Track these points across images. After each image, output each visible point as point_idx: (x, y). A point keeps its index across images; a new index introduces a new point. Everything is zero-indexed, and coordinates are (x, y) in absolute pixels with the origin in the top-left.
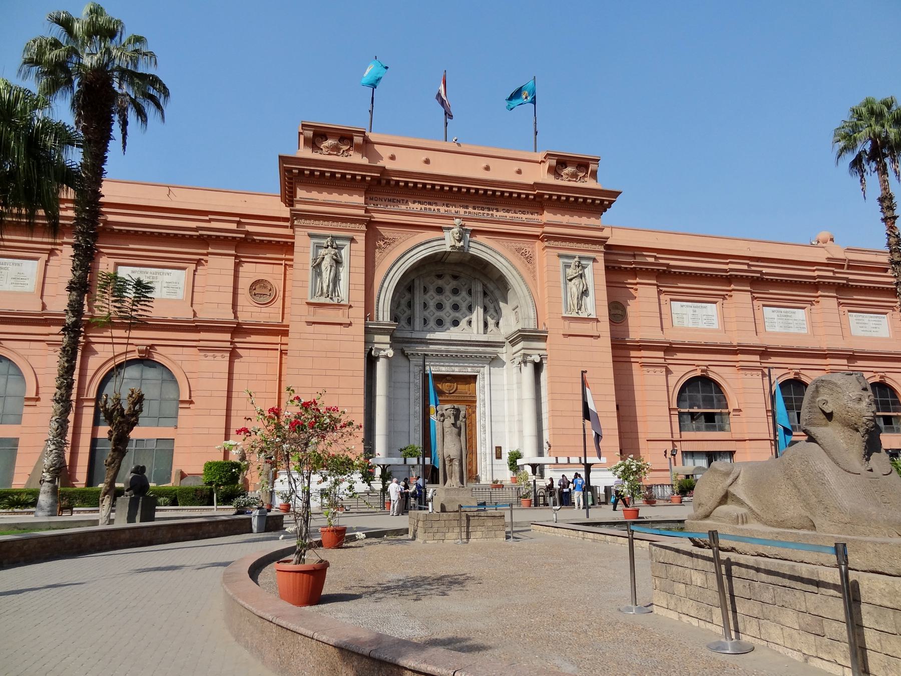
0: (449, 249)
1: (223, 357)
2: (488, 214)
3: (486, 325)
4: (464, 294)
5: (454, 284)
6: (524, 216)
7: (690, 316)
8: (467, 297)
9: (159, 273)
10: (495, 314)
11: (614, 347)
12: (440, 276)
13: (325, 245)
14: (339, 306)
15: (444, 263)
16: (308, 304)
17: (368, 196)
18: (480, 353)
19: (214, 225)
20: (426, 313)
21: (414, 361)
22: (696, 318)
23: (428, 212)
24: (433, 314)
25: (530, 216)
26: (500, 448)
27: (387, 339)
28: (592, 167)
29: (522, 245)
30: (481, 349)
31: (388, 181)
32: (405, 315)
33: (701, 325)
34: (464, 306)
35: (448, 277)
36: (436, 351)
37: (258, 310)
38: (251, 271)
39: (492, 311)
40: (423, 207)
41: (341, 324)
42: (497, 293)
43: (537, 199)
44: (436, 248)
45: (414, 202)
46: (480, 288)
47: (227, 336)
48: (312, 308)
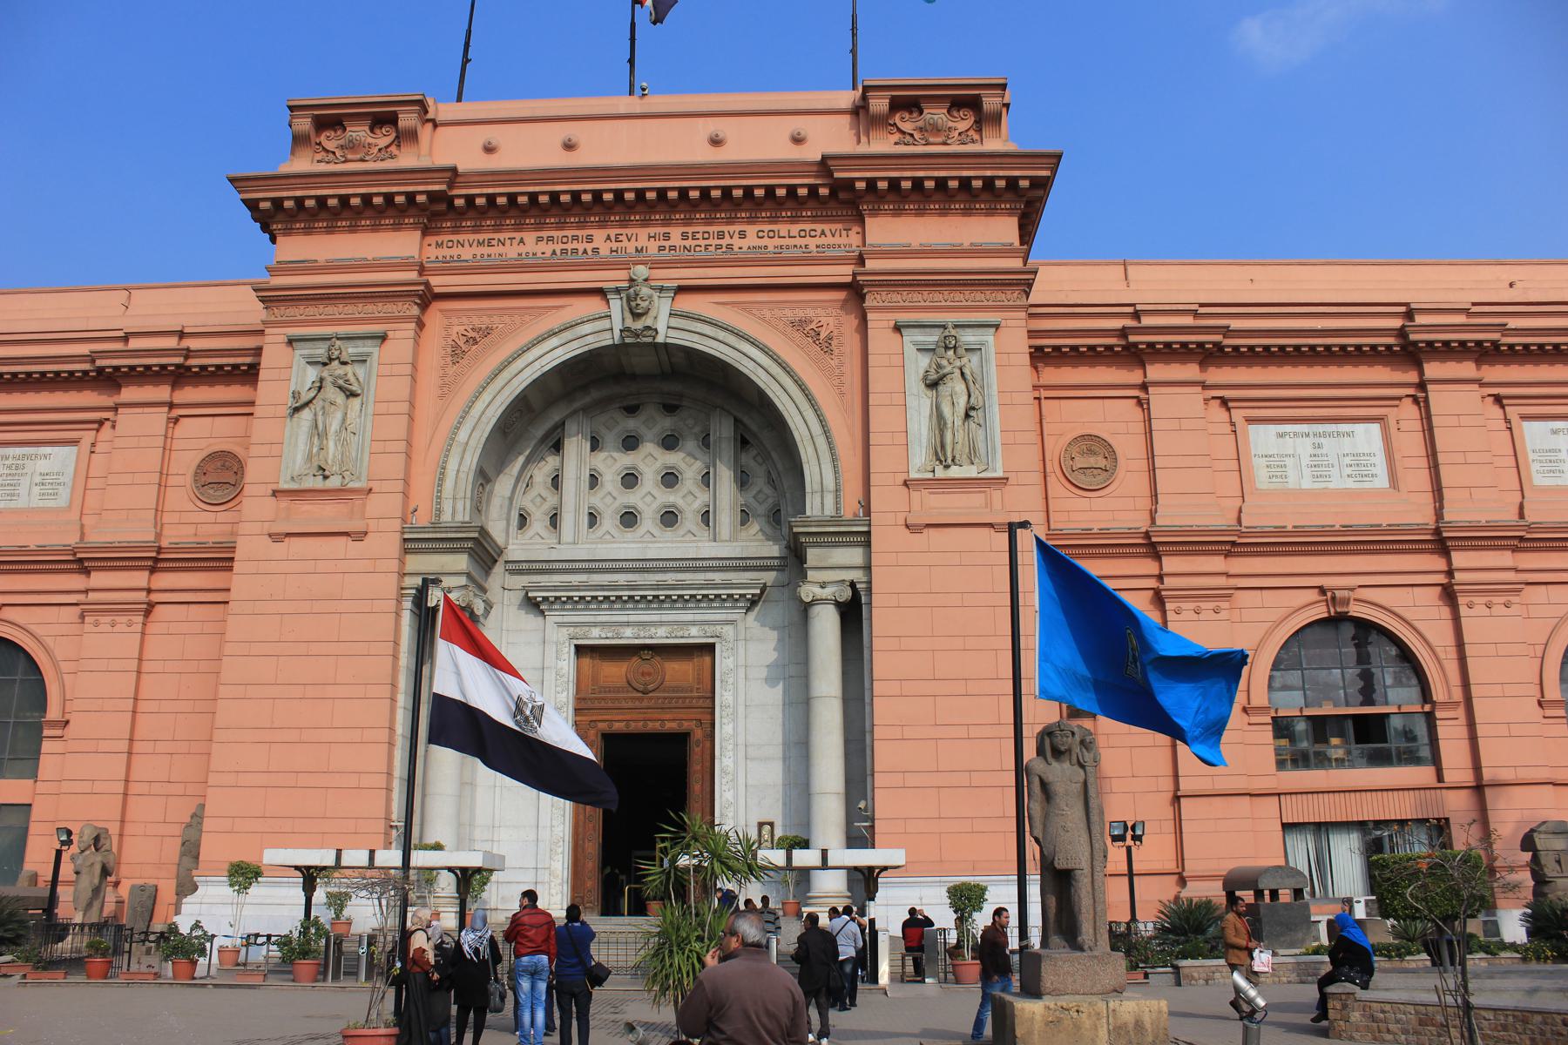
0: (617, 340)
2: (719, 247)
3: (745, 516)
5: (666, 423)
6: (812, 243)
7: (1306, 460)
10: (768, 490)
12: (631, 410)
14: (340, 493)
15: (634, 377)
16: (275, 493)
17: (431, 239)
18: (716, 586)
22: (1325, 463)
23: (570, 258)
24: (612, 498)
25: (829, 240)
26: (771, 824)
29: (810, 313)
30: (717, 577)
31: (470, 199)
33: (1339, 481)
35: (650, 411)
36: (602, 587)
37: (210, 517)
38: (202, 436)
39: (759, 483)
40: (558, 248)
41: (347, 534)
43: (841, 196)
44: (590, 339)
45: (539, 239)
46: (723, 430)
47: (140, 578)
48: (284, 503)
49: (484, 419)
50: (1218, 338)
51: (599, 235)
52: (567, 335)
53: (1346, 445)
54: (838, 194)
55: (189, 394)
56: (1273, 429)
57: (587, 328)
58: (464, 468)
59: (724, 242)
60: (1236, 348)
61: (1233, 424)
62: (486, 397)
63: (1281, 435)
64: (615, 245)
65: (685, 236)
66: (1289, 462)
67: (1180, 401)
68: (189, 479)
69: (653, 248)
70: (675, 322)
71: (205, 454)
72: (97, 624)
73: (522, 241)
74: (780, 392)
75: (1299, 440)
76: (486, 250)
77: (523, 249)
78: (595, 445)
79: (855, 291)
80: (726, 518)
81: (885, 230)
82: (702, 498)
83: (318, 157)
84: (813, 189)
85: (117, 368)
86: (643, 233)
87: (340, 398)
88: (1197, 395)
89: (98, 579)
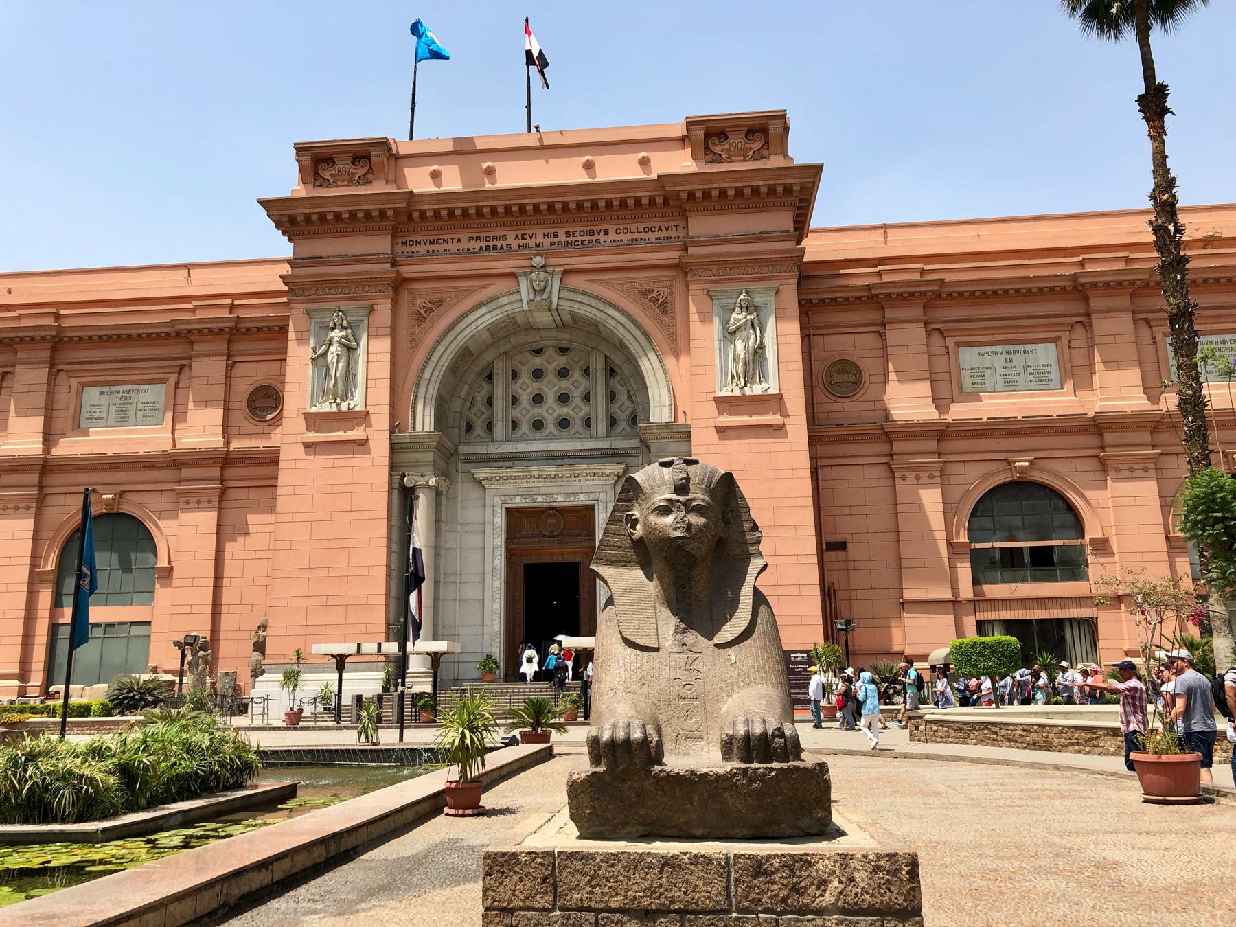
0: (526, 308)
1: (210, 502)
2: (590, 241)
3: (612, 422)
4: (576, 375)
5: (562, 361)
6: (652, 236)
7: (1000, 371)
8: (582, 380)
9: (133, 391)
10: (628, 403)
11: (813, 441)
12: (538, 352)
13: (331, 325)
17: (399, 241)
19: (200, 315)
20: (516, 413)
21: (492, 487)
24: (526, 412)
27: (429, 456)
28: (774, 128)
29: (652, 285)
32: (484, 416)
34: (576, 395)
35: (550, 352)
38: (249, 375)
40: (484, 244)
42: (626, 369)
44: (508, 308)
45: (471, 239)
46: (598, 364)
49: (441, 363)
50: (936, 288)
51: (511, 236)
52: (492, 305)
53: (1030, 359)
54: (666, 202)
55: (239, 347)
56: (976, 350)
57: (505, 300)
58: (429, 396)
59: (594, 238)
60: (950, 295)
61: (947, 348)
62: (441, 349)
63: (981, 354)
64: (521, 242)
65: (567, 234)
66: (987, 373)
67: (907, 336)
68: (244, 405)
69: (547, 241)
70: (564, 294)
71: (253, 387)
72: (187, 502)
73: (459, 240)
74: (632, 340)
75: (995, 357)
76: (435, 247)
77: (460, 246)
78: (515, 375)
79: (681, 268)
80: (600, 425)
81: (700, 225)
82: (584, 410)
83: (318, 183)
84: (652, 201)
85: (189, 331)
86: (540, 233)
87: (345, 349)
88: (919, 331)
89: (186, 473)
